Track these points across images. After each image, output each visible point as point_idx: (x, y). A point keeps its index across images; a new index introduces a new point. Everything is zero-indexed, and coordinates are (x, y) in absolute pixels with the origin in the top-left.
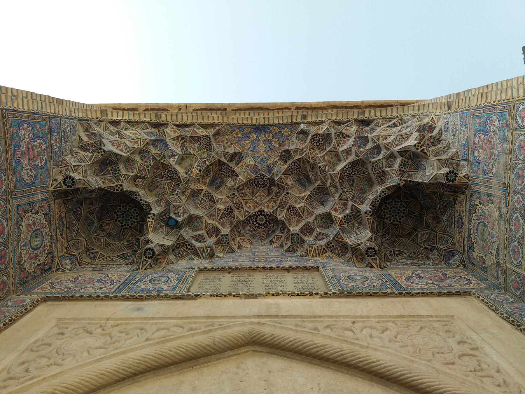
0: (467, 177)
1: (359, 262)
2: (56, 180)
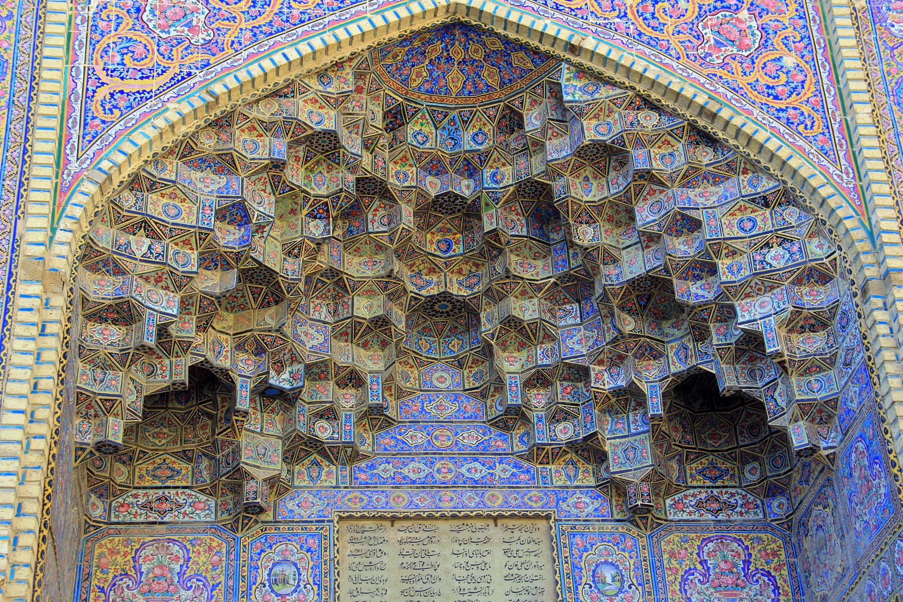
0: (832, 458)
1: (619, 495)
2: (83, 450)
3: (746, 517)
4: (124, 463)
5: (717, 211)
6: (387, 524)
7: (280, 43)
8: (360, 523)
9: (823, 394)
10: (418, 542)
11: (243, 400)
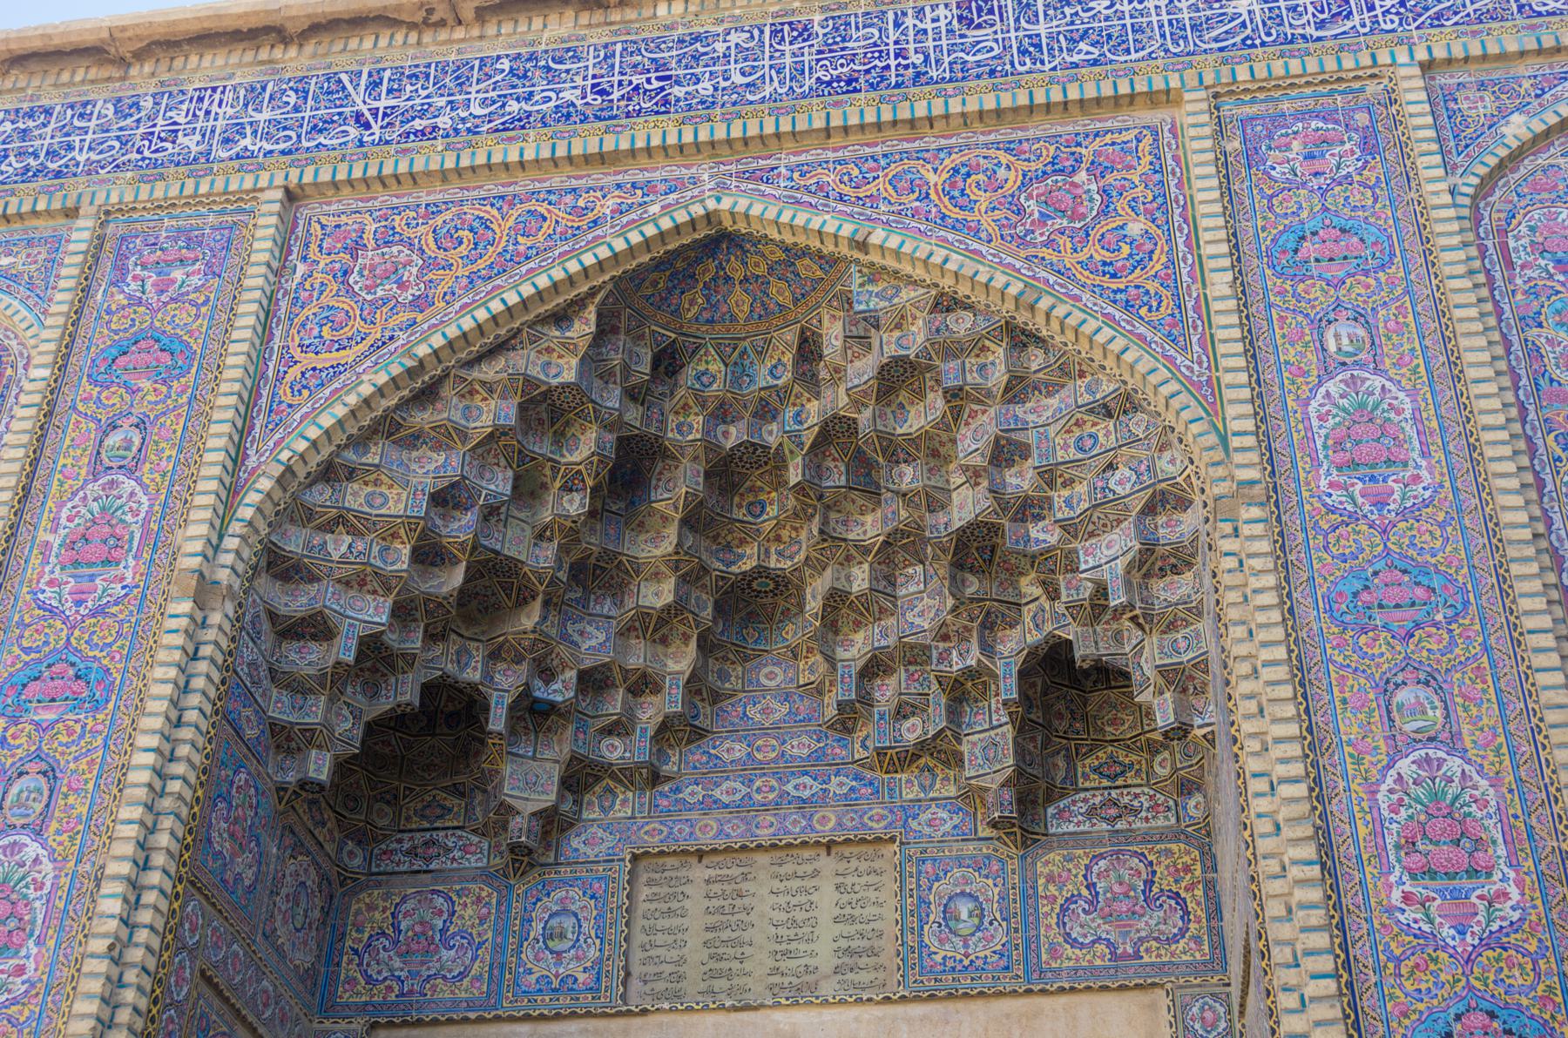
0: (1210, 739)
2: (286, 790)
3: (1153, 823)
4: (388, 803)
5: (1052, 430)
6: (694, 860)
7: (500, 287)
8: (661, 861)
9: (1192, 655)
10: (730, 880)
11: (497, 721)
